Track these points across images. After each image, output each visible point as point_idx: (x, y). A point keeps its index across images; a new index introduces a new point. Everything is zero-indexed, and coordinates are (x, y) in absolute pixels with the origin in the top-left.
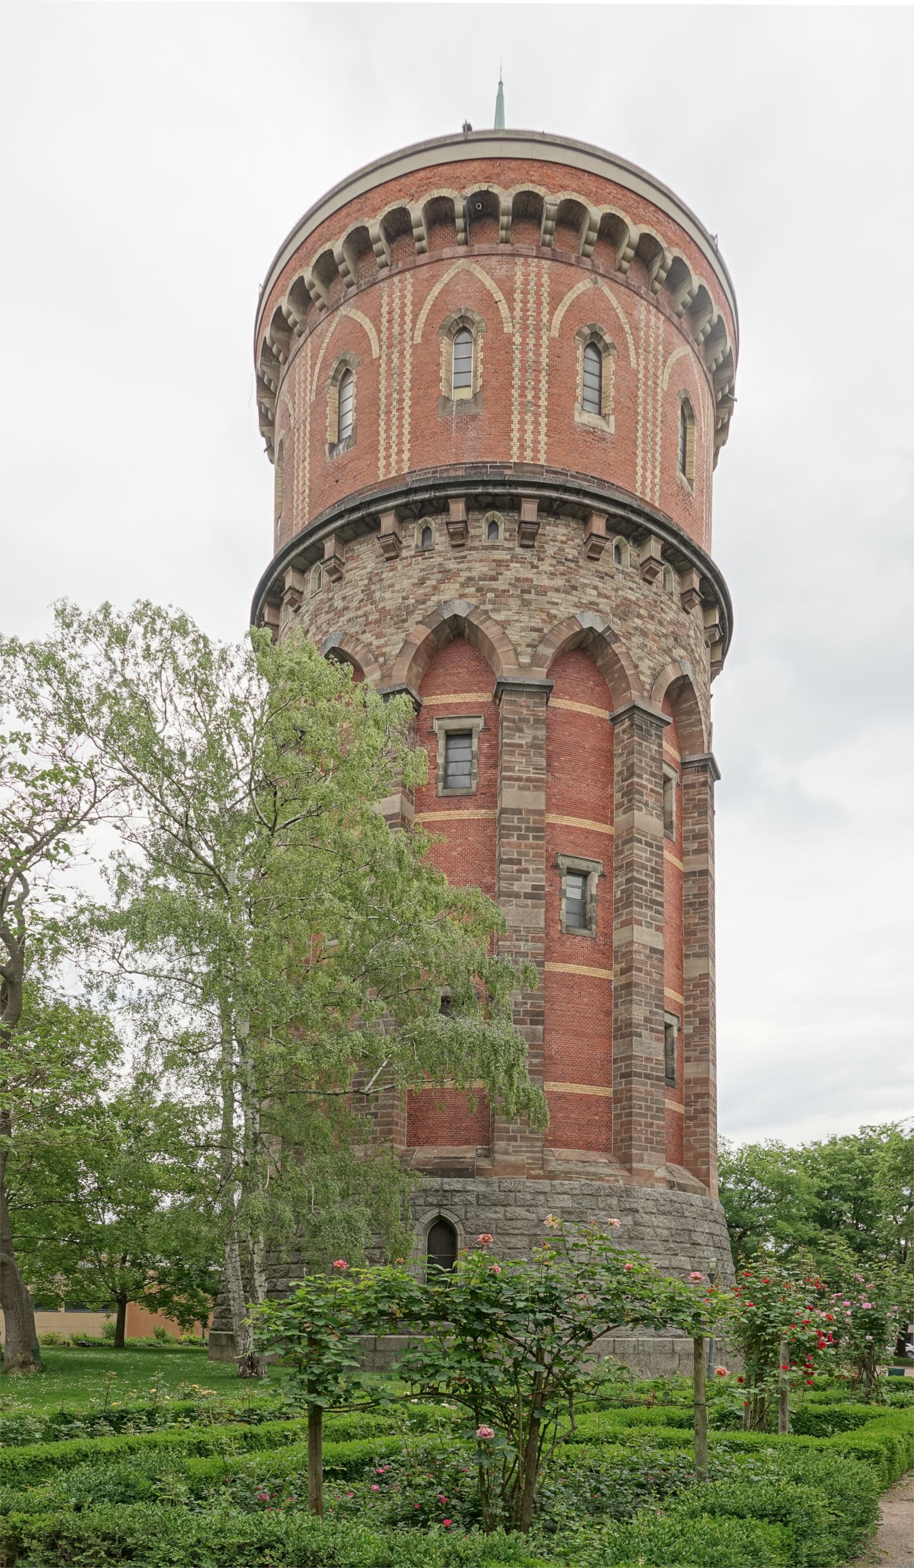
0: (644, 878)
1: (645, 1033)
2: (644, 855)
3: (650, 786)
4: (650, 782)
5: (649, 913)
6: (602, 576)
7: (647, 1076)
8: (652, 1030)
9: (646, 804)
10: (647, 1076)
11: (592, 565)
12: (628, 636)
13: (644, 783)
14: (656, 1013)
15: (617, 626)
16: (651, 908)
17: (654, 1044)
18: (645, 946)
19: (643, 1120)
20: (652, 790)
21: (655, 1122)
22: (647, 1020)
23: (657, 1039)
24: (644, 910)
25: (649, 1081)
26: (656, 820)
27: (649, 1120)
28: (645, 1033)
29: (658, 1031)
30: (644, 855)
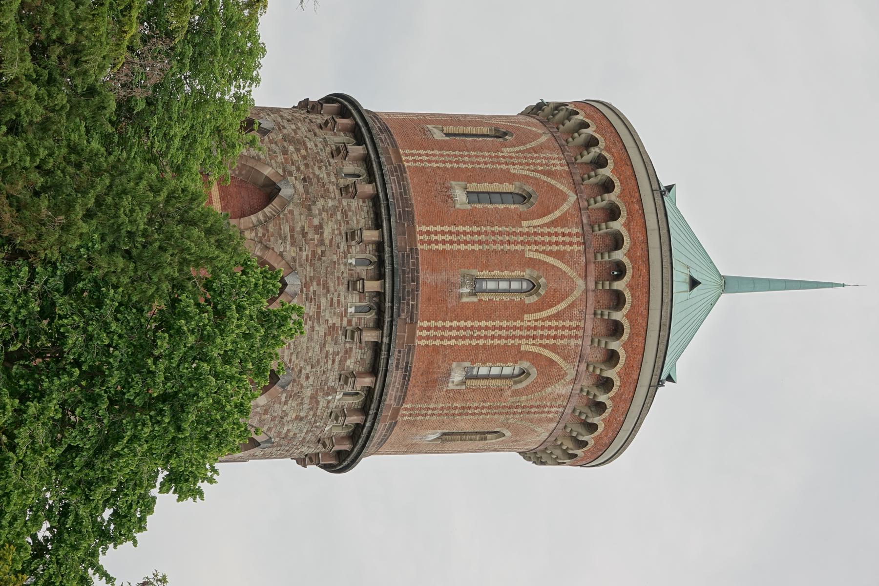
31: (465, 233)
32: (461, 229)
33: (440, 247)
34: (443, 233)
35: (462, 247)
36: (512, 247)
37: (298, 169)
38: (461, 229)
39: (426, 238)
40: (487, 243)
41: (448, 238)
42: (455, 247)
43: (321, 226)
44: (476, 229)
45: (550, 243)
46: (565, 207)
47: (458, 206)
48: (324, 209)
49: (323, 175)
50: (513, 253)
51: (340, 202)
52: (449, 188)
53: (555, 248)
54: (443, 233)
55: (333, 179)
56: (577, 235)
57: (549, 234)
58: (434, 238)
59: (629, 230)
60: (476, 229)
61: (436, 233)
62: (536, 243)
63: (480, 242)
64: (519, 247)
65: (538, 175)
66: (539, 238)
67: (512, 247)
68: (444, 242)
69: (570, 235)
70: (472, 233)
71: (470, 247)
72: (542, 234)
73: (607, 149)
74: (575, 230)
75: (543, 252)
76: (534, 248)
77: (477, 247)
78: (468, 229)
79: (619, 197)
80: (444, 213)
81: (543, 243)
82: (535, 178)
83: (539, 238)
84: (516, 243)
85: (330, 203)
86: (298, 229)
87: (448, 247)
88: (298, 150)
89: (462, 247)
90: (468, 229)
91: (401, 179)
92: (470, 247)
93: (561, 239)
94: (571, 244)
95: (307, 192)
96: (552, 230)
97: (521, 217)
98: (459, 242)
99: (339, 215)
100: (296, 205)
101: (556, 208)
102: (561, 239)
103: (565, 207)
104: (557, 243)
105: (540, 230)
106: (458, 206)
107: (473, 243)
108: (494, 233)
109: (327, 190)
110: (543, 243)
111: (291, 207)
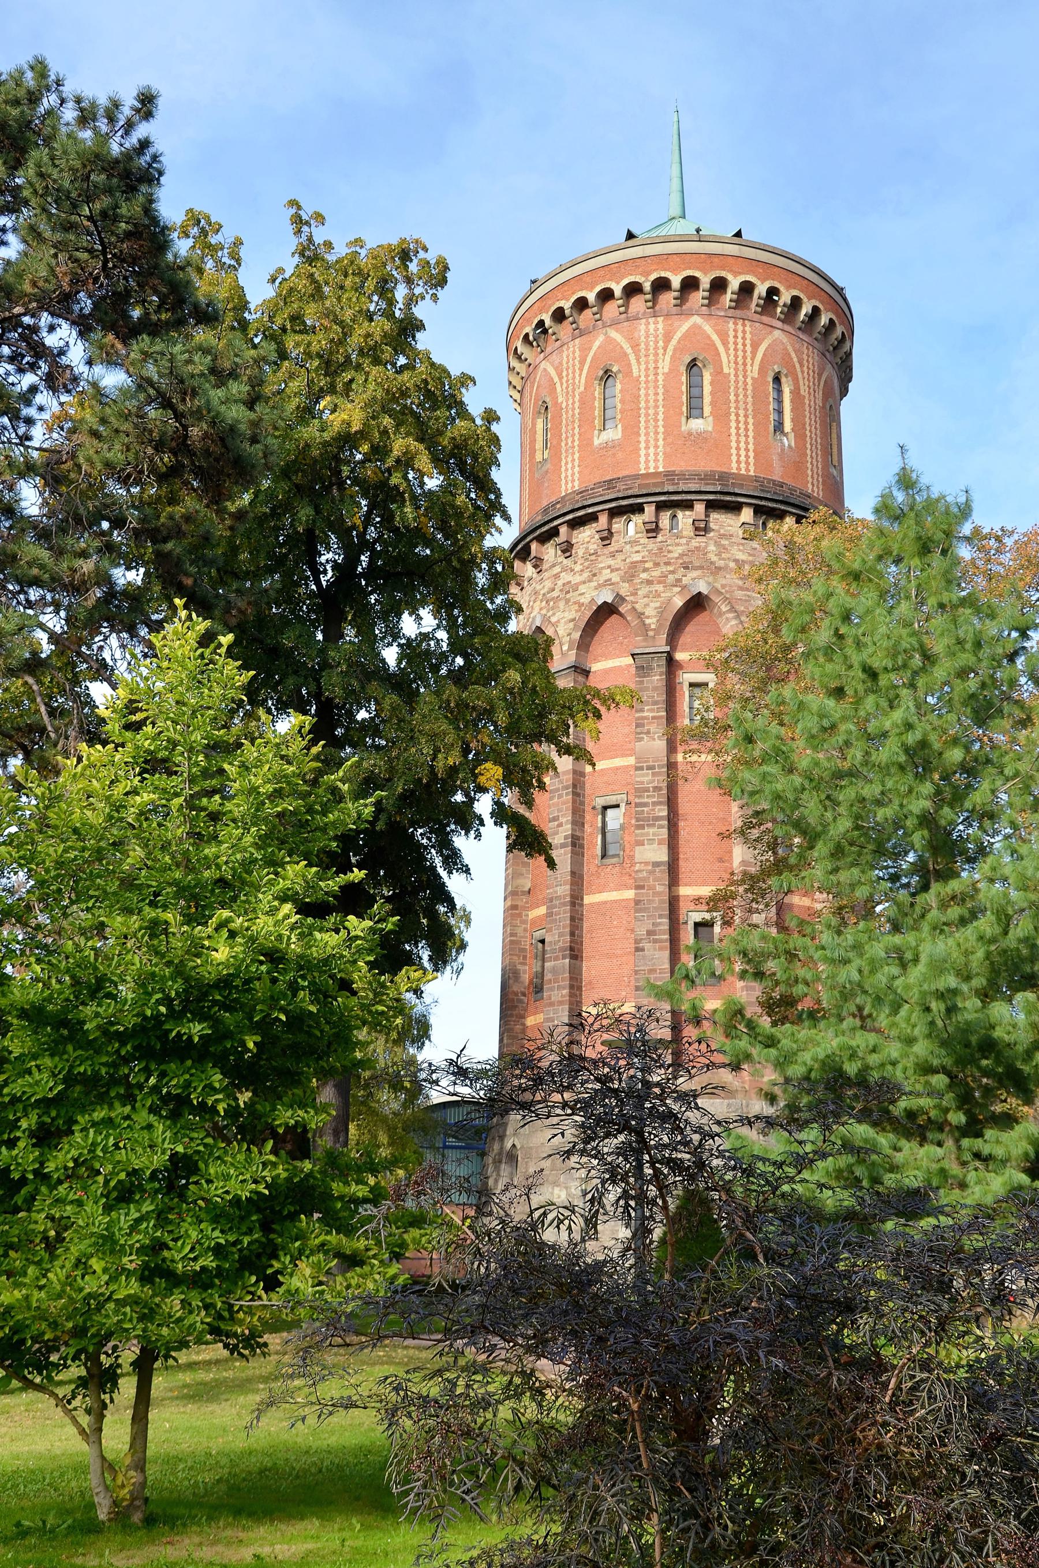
1: (647, 946)
2: (645, 779)
4: (652, 710)
5: (651, 830)
8: (655, 941)
9: (648, 732)
11: (606, 551)
12: (634, 594)
13: (646, 714)
14: (660, 924)
15: (624, 589)
16: (654, 825)
17: (657, 954)
18: (646, 863)
20: (653, 718)
22: (649, 933)
23: (661, 949)
28: (647, 946)
29: (661, 941)
30: (645, 779)
31: (738, 428)
32: (733, 431)
33: (751, 454)
34: (738, 449)
35: (751, 434)
36: (750, 387)
37: (672, 572)
38: (733, 431)
39: (743, 465)
40: (746, 410)
41: (742, 445)
42: (751, 440)
43: (736, 561)
44: (733, 417)
45: (744, 351)
46: (708, 329)
47: (710, 429)
48: (719, 554)
49: (679, 550)
50: (754, 390)
51: (711, 539)
52: (690, 434)
53: (749, 348)
54: (738, 449)
55: (684, 541)
56: (735, 324)
57: (736, 350)
58: (743, 458)
59: (740, 273)
60: (733, 417)
61: (739, 455)
62: (745, 364)
63: (746, 416)
64: (749, 381)
65: (671, 348)
66: (740, 360)
67: (750, 387)
68: (747, 450)
69: (735, 331)
70: (738, 422)
71: (751, 427)
72: (736, 356)
73: (646, 274)
74: (731, 325)
75: (753, 359)
76: (749, 368)
77: (751, 420)
78: (733, 425)
79: (705, 274)
80: (717, 443)
81: (744, 357)
82: (675, 350)
83: (740, 360)
84: (745, 383)
85: (712, 548)
86: (740, 583)
87: (751, 447)
88: (645, 570)
89: (751, 434)
90: (733, 425)
91: (682, 476)
92: (751, 427)
93: (740, 340)
94: (744, 332)
95: (701, 568)
96: (732, 346)
97: (718, 372)
98: (747, 436)
99: (724, 542)
100: (715, 580)
101: (709, 337)
102: (740, 340)
103: (708, 329)
104: (744, 345)
105: (732, 357)
106: (710, 429)
107: (746, 423)
108: (737, 401)
109: (698, 548)
110: (744, 357)
111: (719, 586)
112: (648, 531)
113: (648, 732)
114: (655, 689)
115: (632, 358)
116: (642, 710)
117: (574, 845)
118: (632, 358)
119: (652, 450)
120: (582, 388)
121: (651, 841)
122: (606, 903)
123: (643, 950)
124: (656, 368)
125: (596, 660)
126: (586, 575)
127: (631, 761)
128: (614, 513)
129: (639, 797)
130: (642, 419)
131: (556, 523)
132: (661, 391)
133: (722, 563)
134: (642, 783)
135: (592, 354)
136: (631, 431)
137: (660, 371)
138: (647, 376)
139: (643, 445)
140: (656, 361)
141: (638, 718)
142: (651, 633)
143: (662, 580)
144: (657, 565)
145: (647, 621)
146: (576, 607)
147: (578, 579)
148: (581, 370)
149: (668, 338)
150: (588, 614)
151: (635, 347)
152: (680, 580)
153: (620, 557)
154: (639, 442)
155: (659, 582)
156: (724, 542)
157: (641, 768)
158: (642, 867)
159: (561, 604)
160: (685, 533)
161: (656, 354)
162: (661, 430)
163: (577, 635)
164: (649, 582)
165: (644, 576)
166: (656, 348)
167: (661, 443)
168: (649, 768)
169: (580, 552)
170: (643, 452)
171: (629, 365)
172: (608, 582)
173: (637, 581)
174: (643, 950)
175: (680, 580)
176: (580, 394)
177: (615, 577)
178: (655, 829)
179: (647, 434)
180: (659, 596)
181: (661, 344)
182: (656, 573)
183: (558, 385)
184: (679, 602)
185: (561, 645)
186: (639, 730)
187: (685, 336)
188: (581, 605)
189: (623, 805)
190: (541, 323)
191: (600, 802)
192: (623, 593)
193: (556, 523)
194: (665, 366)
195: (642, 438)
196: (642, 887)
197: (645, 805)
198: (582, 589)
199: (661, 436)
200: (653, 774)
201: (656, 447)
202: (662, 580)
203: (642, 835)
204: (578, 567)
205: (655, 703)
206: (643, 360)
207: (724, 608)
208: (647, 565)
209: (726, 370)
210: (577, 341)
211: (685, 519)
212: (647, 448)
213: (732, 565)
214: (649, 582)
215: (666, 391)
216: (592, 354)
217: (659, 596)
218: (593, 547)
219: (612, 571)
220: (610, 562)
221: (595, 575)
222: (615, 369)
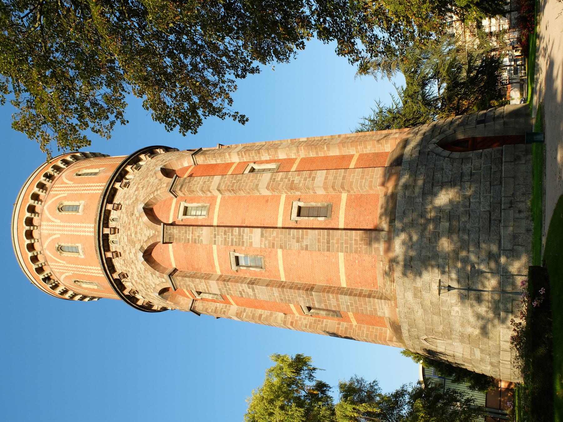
0: (230, 240)
1: (305, 243)
2: (220, 239)
3: (191, 235)
5: (245, 237)
6: (125, 251)
7: (328, 242)
8: (303, 238)
9: (199, 236)
10: (328, 242)
12: (140, 241)
13: (190, 238)
14: (293, 235)
15: (138, 246)
16: (243, 236)
17: (310, 237)
18: (261, 241)
19: (354, 246)
20: (192, 234)
21: (354, 238)
22: (298, 241)
23: (307, 235)
24: (245, 240)
25: (331, 241)
26: (204, 230)
27: (353, 242)
28: (305, 243)
29: (303, 234)
37: (133, 221)
48: (131, 199)
49: (125, 217)
55: (122, 215)
73: (23, 227)
82: (53, 217)
85: (127, 202)
86: (144, 189)
95: (134, 207)
97: (65, 198)
99: (126, 197)
109: (126, 208)
112: (114, 233)
113: (199, 236)
114: (180, 232)
115: (53, 237)
116: (189, 239)
117: (253, 284)
118: (53, 237)
119: (87, 229)
120: (64, 262)
121: (250, 238)
122: (284, 268)
123: (307, 246)
124: (58, 226)
125: (171, 265)
126: (133, 266)
127: (214, 247)
128: (107, 248)
129: (228, 243)
130: (75, 233)
131: (112, 280)
132: (66, 224)
133: (134, 197)
134: (222, 241)
135: (52, 257)
136: (79, 238)
137: (59, 224)
138: (60, 230)
139: (84, 234)
140: (56, 226)
141: (192, 241)
142: (157, 233)
143: (135, 226)
144: (129, 229)
145: (152, 235)
146: (146, 272)
147: (135, 270)
148: (59, 262)
149: (49, 220)
150: (148, 266)
151: (50, 235)
152: (137, 217)
153: (125, 248)
154: (83, 235)
155: (136, 228)
156: (126, 197)
157: (215, 241)
158: (263, 243)
159: (147, 281)
160: (119, 215)
161: (53, 226)
162: (79, 225)
163: (157, 273)
164: (136, 233)
165: (133, 235)
166: (51, 226)
167: (84, 225)
168: (215, 237)
169: (125, 268)
170: (87, 234)
171: (56, 238)
172: (135, 254)
173: (135, 240)
174: (307, 246)
175: (137, 217)
176: (67, 263)
177: (133, 251)
178: (245, 235)
179: (80, 231)
180: (142, 228)
181: (50, 223)
182: (132, 229)
183: (67, 274)
184: (145, 218)
185: (163, 282)
186: (197, 242)
187: (50, 213)
188: (145, 270)
189: (237, 254)
190: (44, 280)
191: (234, 267)
192: (139, 247)
193: (112, 280)
194: (58, 222)
195: (82, 234)
196: (273, 244)
197: (232, 240)
198: (139, 269)
199: (82, 225)
200: (218, 235)
201: (85, 227)
202: (135, 226)
203: (247, 242)
204: (130, 270)
205: (186, 232)
206: (55, 232)
207: (152, 196)
208: (129, 234)
209: (66, 195)
210: (49, 263)
211: (114, 214)
212: (85, 232)
213: (136, 193)
214: (136, 233)
215: (67, 222)
216: (52, 257)
217: (142, 228)
218: (122, 262)
219: (131, 252)
220: (127, 252)
221: (133, 261)
222: (57, 246)
